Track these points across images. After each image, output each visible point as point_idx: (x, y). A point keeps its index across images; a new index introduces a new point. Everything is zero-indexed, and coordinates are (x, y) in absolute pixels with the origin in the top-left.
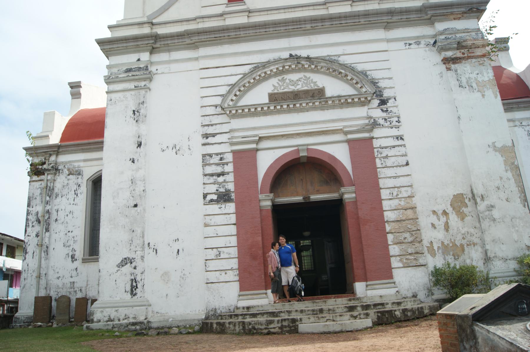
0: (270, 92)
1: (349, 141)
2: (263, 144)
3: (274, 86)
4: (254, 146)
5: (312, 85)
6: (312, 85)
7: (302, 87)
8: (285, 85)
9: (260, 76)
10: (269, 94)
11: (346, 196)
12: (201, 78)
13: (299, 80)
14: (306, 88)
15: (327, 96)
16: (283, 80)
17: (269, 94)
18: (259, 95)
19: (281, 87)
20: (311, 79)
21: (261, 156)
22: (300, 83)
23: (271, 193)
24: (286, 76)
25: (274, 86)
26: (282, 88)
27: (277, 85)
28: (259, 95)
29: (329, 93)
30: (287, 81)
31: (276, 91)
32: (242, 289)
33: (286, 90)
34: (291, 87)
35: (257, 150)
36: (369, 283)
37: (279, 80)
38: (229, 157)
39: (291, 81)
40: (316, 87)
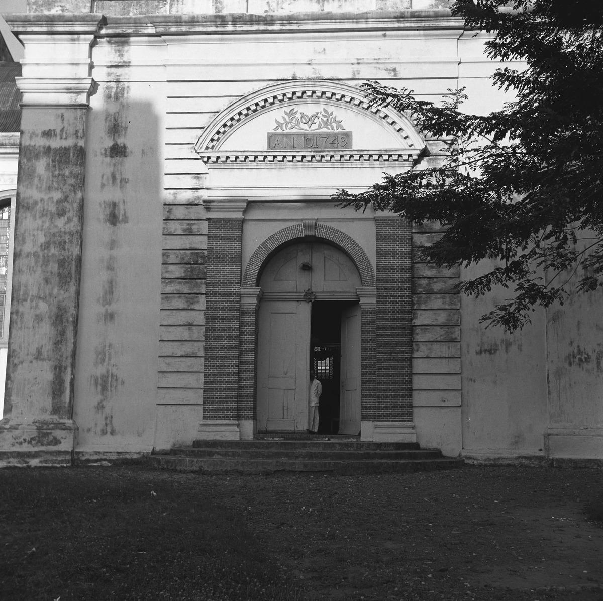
0: (272, 131)
1: (376, 219)
2: (255, 214)
4: (239, 215)
5: (334, 125)
6: (334, 125)
7: (320, 127)
8: (294, 121)
10: (269, 133)
12: (168, 97)
13: (315, 116)
14: (324, 130)
16: (292, 113)
17: (269, 133)
18: (252, 136)
19: (287, 124)
20: (333, 116)
21: (249, 228)
22: (316, 120)
24: (296, 108)
26: (290, 126)
27: (282, 121)
28: (252, 136)
29: (358, 143)
30: (298, 115)
31: (280, 131)
32: (204, 417)
33: (294, 130)
34: (302, 125)
35: (243, 221)
36: (379, 423)
37: (286, 113)
38: (204, 227)
40: (340, 130)
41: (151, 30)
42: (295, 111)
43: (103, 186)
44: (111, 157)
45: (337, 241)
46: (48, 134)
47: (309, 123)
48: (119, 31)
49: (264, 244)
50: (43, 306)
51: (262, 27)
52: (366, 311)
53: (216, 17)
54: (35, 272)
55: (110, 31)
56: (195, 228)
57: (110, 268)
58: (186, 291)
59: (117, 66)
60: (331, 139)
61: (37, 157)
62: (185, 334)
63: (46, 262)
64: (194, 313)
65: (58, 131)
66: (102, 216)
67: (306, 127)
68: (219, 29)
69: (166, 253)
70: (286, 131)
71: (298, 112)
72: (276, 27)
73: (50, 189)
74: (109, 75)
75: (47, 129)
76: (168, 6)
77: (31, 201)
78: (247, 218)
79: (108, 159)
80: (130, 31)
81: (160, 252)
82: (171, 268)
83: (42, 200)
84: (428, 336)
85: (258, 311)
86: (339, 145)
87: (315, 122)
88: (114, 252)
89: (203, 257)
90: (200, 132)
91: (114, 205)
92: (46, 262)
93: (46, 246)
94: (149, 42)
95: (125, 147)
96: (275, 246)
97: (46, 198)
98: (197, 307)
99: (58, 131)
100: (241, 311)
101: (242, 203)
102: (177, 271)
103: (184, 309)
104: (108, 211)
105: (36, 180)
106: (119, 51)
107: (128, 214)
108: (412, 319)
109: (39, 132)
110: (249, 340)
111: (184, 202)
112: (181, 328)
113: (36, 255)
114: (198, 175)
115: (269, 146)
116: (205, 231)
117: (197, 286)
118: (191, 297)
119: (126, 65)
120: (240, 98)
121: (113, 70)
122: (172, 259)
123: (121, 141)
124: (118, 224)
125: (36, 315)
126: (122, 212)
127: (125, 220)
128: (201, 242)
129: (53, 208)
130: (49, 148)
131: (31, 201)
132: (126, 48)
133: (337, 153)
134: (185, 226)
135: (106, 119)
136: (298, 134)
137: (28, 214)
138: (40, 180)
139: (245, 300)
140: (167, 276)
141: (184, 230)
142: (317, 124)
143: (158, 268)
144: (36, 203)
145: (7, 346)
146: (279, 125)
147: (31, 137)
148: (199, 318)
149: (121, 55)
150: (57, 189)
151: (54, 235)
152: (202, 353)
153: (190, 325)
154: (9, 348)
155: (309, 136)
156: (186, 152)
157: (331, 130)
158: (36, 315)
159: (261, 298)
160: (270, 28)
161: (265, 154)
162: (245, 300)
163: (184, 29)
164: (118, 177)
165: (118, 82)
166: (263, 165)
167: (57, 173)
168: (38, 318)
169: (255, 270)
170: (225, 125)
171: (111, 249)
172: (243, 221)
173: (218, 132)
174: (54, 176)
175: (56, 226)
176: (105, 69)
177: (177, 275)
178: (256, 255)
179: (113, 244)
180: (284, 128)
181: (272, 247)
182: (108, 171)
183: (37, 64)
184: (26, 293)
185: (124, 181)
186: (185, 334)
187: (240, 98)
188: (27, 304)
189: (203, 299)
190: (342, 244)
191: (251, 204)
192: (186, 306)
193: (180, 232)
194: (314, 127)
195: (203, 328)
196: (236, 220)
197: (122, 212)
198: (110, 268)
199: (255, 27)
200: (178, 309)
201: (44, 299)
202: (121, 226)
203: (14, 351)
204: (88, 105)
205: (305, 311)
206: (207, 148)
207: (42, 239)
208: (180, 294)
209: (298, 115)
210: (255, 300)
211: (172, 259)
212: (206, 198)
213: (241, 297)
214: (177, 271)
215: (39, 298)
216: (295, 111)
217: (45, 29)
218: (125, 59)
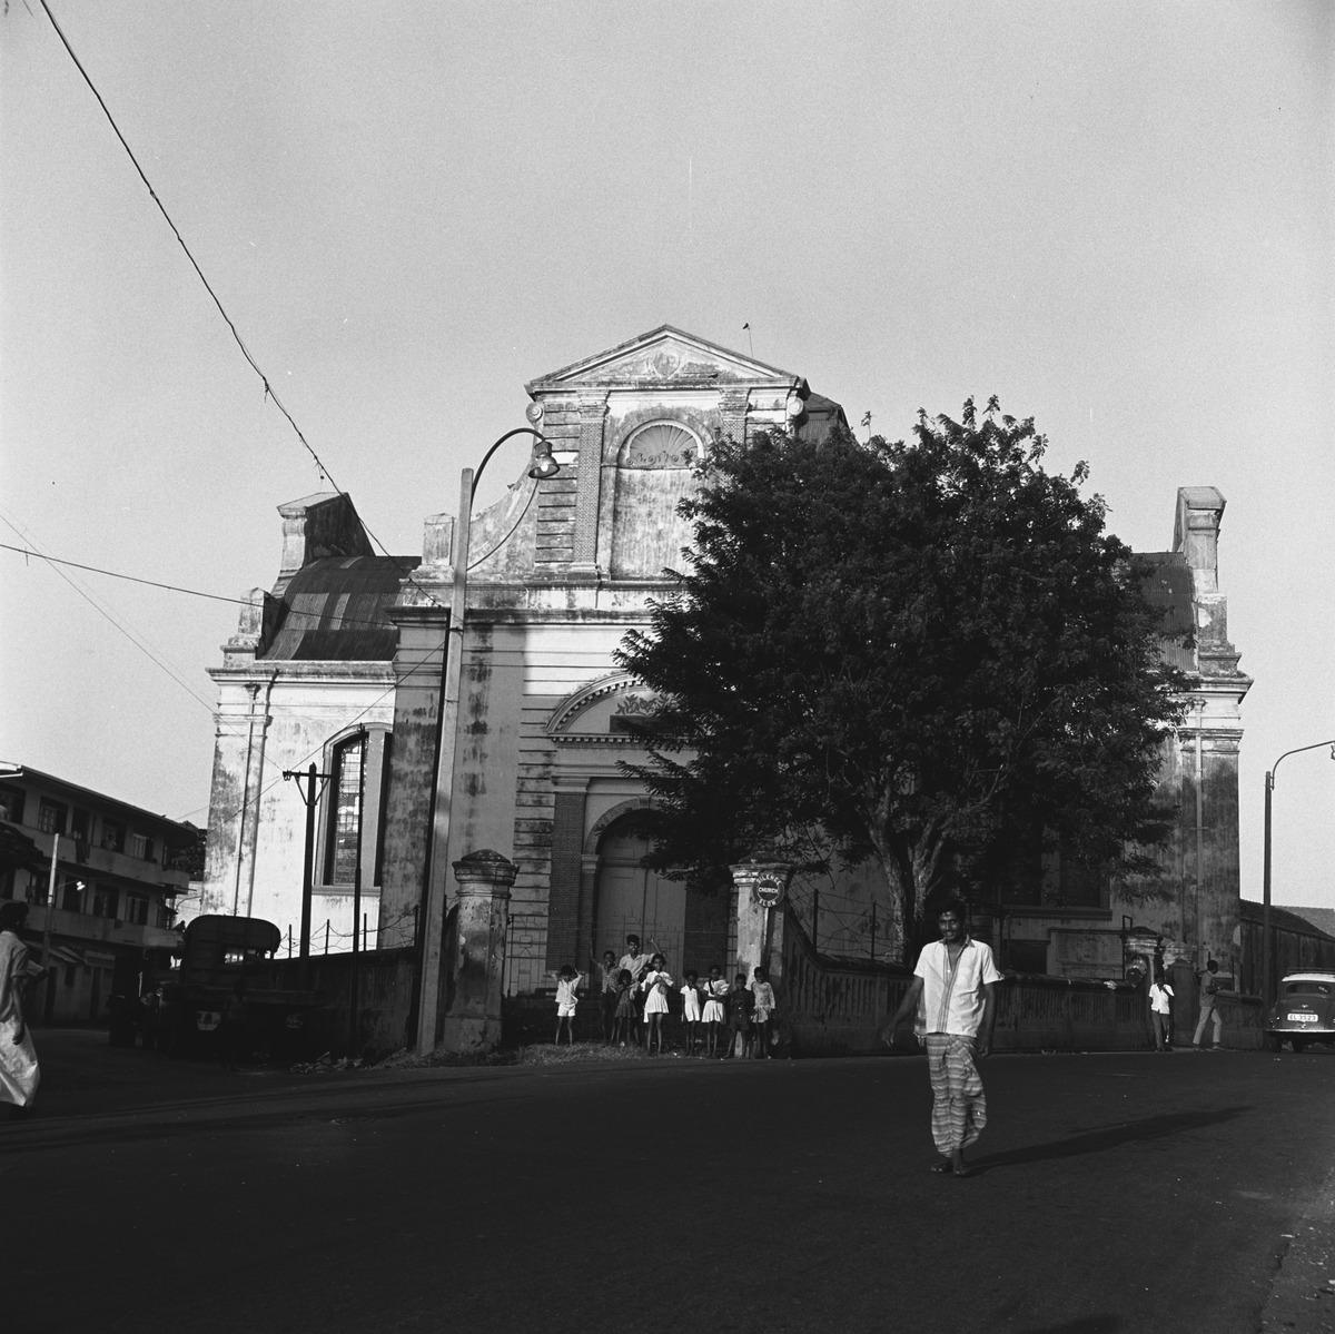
2: (598, 789)
4: (583, 790)
10: (611, 717)
17: (611, 717)
27: (623, 705)
31: (621, 714)
33: (634, 714)
35: (586, 795)
41: (511, 621)
43: (465, 759)
44: (473, 733)
46: (418, 712)
48: (482, 620)
49: (604, 815)
50: (410, 868)
51: (608, 621)
53: (567, 611)
54: (404, 837)
55: (475, 621)
56: (544, 800)
57: (469, 834)
59: (480, 651)
61: (409, 733)
62: (532, 895)
63: (413, 829)
64: (540, 877)
65: (427, 710)
66: (463, 787)
67: (644, 711)
68: (570, 622)
69: (518, 822)
73: (418, 762)
74: (473, 658)
75: (418, 708)
76: (527, 596)
77: (402, 773)
78: (591, 792)
79: (470, 735)
80: (493, 621)
81: (514, 821)
82: (522, 835)
83: (412, 772)
85: (598, 875)
88: (473, 821)
89: (550, 827)
90: (551, 713)
91: (474, 777)
92: (413, 829)
93: (414, 814)
94: (510, 629)
95: (485, 725)
96: (614, 817)
97: (416, 770)
98: (544, 871)
99: (427, 710)
100: (582, 875)
102: (527, 839)
103: (532, 873)
104: (468, 783)
105: (407, 753)
106: (483, 637)
107: (486, 786)
109: (411, 710)
110: (589, 903)
112: (529, 890)
113: (405, 821)
114: (548, 753)
115: (613, 729)
116: (553, 804)
117: (544, 852)
118: (539, 863)
119: (489, 650)
121: (478, 654)
122: (523, 827)
123: (481, 719)
124: (477, 795)
125: (405, 876)
126: (480, 783)
127: (484, 791)
128: (549, 813)
129: (421, 780)
130: (419, 725)
131: (402, 773)
132: (489, 634)
134: (536, 799)
135: (469, 699)
137: (400, 785)
138: (411, 754)
139: (586, 867)
140: (519, 842)
141: (534, 802)
143: (511, 835)
144: (406, 774)
146: (621, 709)
147: (403, 715)
148: (545, 881)
149: (485, 641)
150: (425, 763)
151: (421, 804)
152: (546, 913)
153: (537, 887)
154: (381, 901)
156: (538, 731)
158: (405, 876)
159: (602, 865)
160: (615, 621)
162: (586, 867)
163: (540, 620)
164: (479, 752)
165: (481, 665)
166: (605, 746)
167: (425, 748)
168: (406, 878)
169: (595, 840)
170: (572, 709)
171: (470, 817)
172: (586, 795)
173: (567, 715)
174: (422, 751)
175: (423, 796)
176: (470, 654)
177: (528, 842)
178: (597, 828)
179: (472, 813)
182: (470, 746)
183: (412, 649)
184: (396, 856)
185: (484, 756)
186: (532, 895)
188: (397, 865)
189: (549, 864)
191: (594, 780)
192: (533, 870)
193: (530, 803)
195: (548, 891)
196: (580, 794)
197: (480, 783)
198: (469, 834)
199: (602, 621)
200: (527, 873)
201: (411, 861)
202: (480, 797)
203: (385, 907)
206: (557, 729)
207: (411, 808)
208: (529, 859)
210: (594, 867)
211: (523, 827)
212: (554, 774)
213: (582, 863)
214: (527, 839)
215: (407, 860)
217: (419, 619)
218: (488, 645)
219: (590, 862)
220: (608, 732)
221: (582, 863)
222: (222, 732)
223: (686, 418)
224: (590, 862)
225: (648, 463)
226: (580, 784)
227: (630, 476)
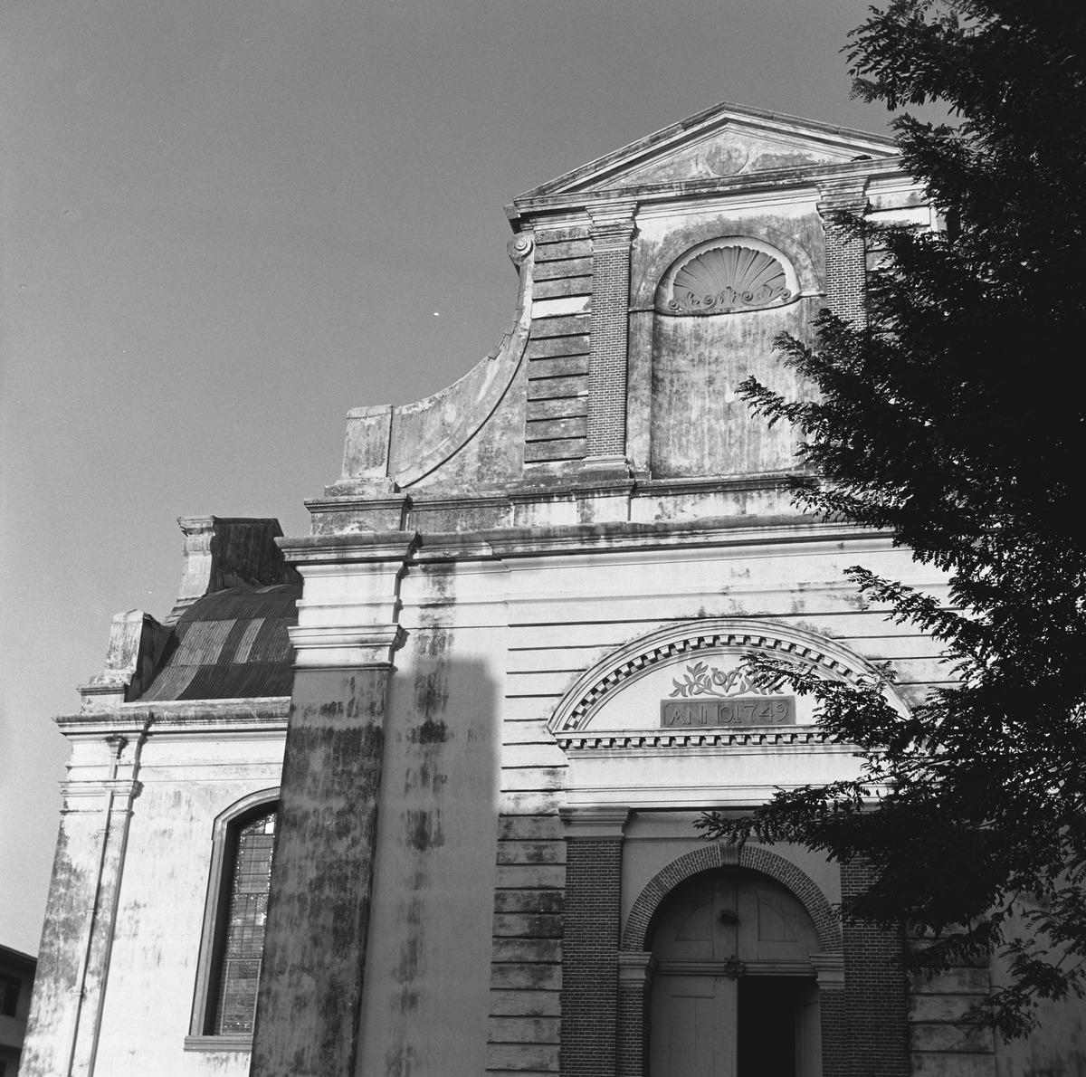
3: (675, 683)
4: (617, 832)
7: (743, 690)
8: (702, 682)
9: (644, 657)
10: (663, 702)
11: (822, 977)
12: (510, 650)
15: (799, 722)
16: (698, 670)
17: (663, 702)
18: (636, 708)
22: (737, 680)
23: (645, 950)
24: (705, 662)
25: (675, 683)
27: (683, 682)
28: (636, 708)
30: (709, 673)
31: (680, 697)
33: (703, 696)
34: (715, 688)
35: (623, 842)
37: (689, 669)
38: (561, 850)
39: (716, 672)
41: (486, 552)
42: (703, 666)
43: (408, 787)
44: (422, 742)
45: (776, 875)
46: (330, 710)
47: (727, 684)
48: (439, 554)
49: (656, 879)
50: (308, 983)
51: (651, 541)
52: (827, 994)
53: (581, 529)
54: (299, 926)
55: (427, 555)
56: (547, 853)
57: (413, 919)
58: (531, 958)
59: (435, 606)
60: (761, 710)
61: (312, 745)
62: (526, 1031)
63: (316, 912)
64: (544, 996)
65: (345, 705)
66: (404, 836)
67: (720, 690)
68: (586, 547)
69: (501, 895)
70: (689, 697)
71: (709, 668)
72: (672, 541)
73: (328, 794)
74: (423, 618)
75: (330, 702)
76: (512, 515)
77: (299, 814)
78: (628, 837)
79: (417, 746)
80: (455, 554)
81: (493, 893)
82: (508, 919)
83: (316, 811)
84: (937, 1042)
85: (649, 992)
86: (775, 720)
87: (735, 682)
88: (422, 894)
89: (559, 901)
90: (557, 700)
91: (423, 817)
92: (316, 912)
93: (318, 884)
94: (484, 568)
95: (443, 727)
96: (675, 882)
97: (322, 808)
98: (548, 985)
99: (345, 705)
100: (621, 993)
101: (622, 813)
102: (518, 925)
104: (413, 827)
105: (309, 780)
106: (439, 583)
107: (445, 831)
108: (907, 1011)
109: (318, 707)
110: (634, 1045)
111: (531, 812)
112: (521, 1022)
113: (301, 898)
114: (552, 770)
116: (563, 859)
117: (549, 949)
118: (539, 970)
119: (449, 603)
120: (619, 648)
121: (430, 611)
122: (511, 904)
123: (437, 717)
124: (428, 848)
125: (298, 998)
126: (434, 828)
127: (440, 841)
128: (555, 877)
129: (330, 823)
130: (331, 731)
131: (299, 814)
132: (449, 578)
133: (770, 732)
134: (532, 851)
135: (416, 685)
136: (709, 702)
137: (294, 834)
138: (315, 780)
139: (627, 975)
140: (502, 932)
141: (530, 857)
142: (739, 686)
143: (486, 922)
144: (306, 816)
145: (251, 1047)
146: (679, 688)
147: (305, 715)
148: (551, 1004)
149: (442, 589)
150: (339, 794)
151: (331, 866)
152: (555, 1066)
153: (536, 1016)
154: (253, 1052)
155: (726, 705)
156: (535, 732)
157: (761, 695)
158: (298, 998)
159: (655, 972)
160: (663, 542)
161: (657, 735)
162: (627, 975)
163: (534, 548)
164: (431, 774)
165: (436, 628)
166: (654, 751)
167: (340, 769)
168: (300, 1002)
169: (642, 924)
170: (594, 691)
171: (416, 888)
172: (623, 842)
173: (584, 702)
174: (335, 774)
175: (334, 852)
176: (418, 610)
177: (518, 931)
178: (644, 897)
179: (419, 880)
180: (687, 693)
181: (670, 884)
182: (416, 765)
183: (320, 607)
184: (283, 961)
185: (440, 779)
186: (526, 1031)
187: (619, 648)
188: (285, 979)
189: (557, 971)
190: (785, 879)
191: (633, 815)
192: (530, 984)
193: (523, 859)
194: (733, 690)
195: (558, 1022)
196: (610, 840)
197: (434, 828)
198: (413, 919)
199: (640, 542)
200: (519, 989)
201: (309, 971)
202: (435, 851)
203: (261, 1057)
204: (391, 665)
205: (727, 993)
206: (567, 726)
207: (312, 874)
208: (522, 963)
209: (709, 673)
210: (641, 975)
211: (511, 904)
212: (564, 805)
213: (619, 968)
214: (518, 925)
215: (303, 969)
216: (703, 666)
217: (333, 556)
218: (448, 594)
219: (634, 966)
220: (658, 727)
221: (619, 968)
222: (71, 808)
223: (764, 231)
224: (634, 966)
225: (703, 307)
226: (610, 822)
227: (676, 327)
